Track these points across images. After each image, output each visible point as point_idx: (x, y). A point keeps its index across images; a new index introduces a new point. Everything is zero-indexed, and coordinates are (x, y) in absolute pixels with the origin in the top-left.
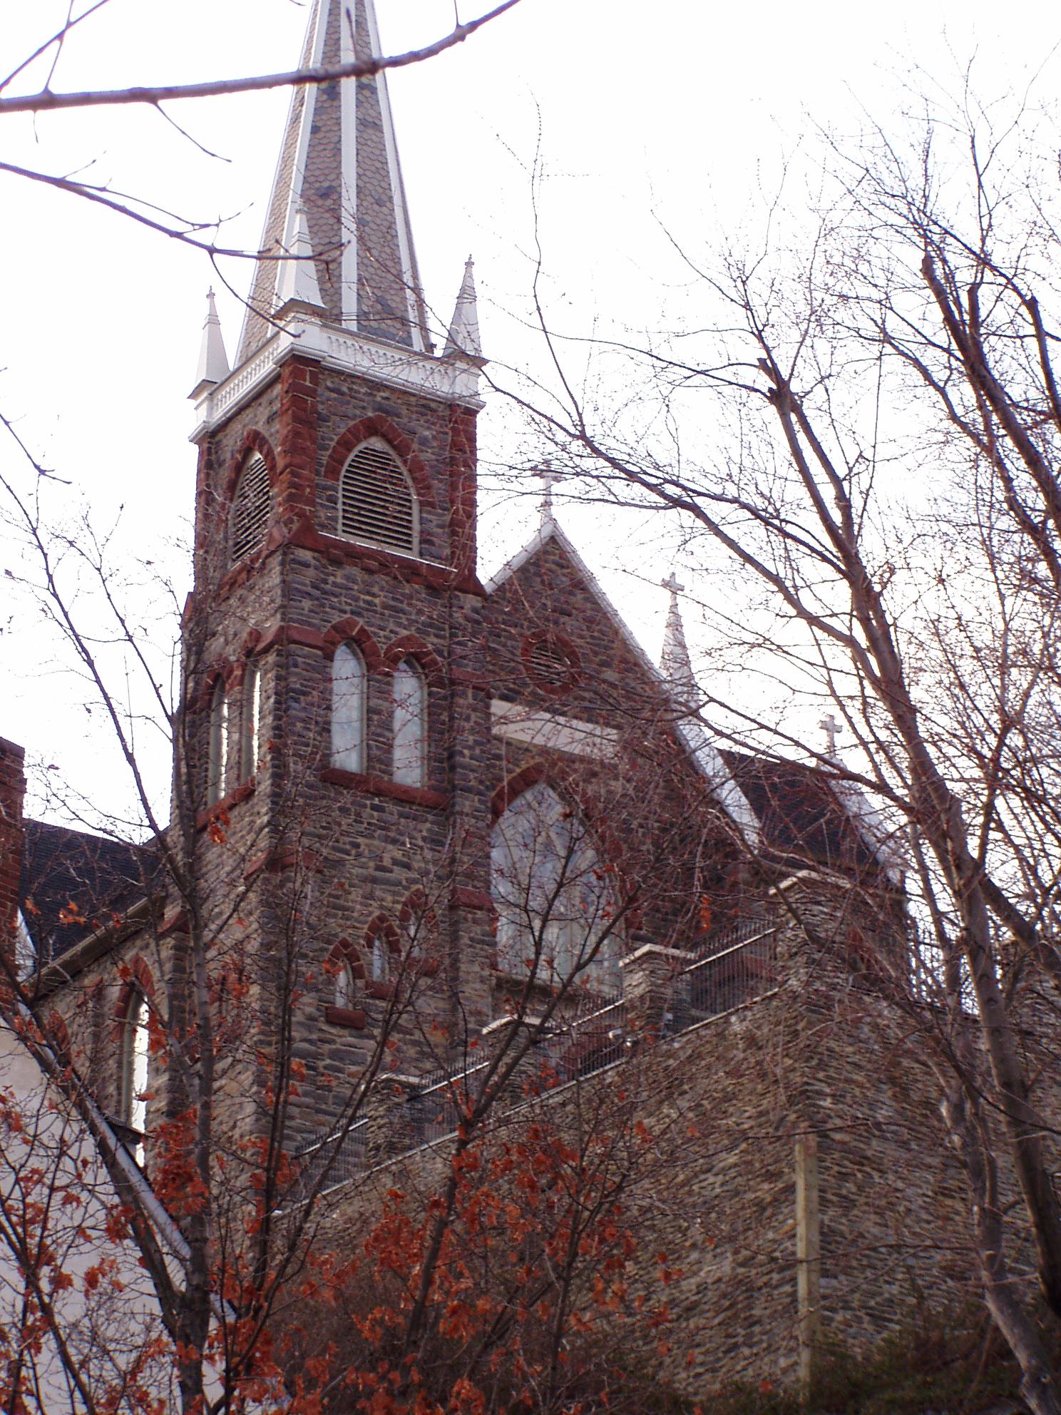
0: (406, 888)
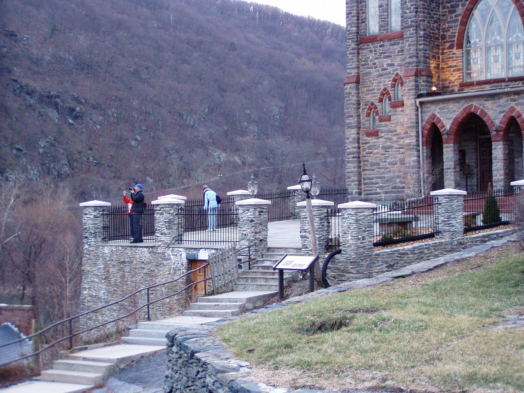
0: (392, 74)
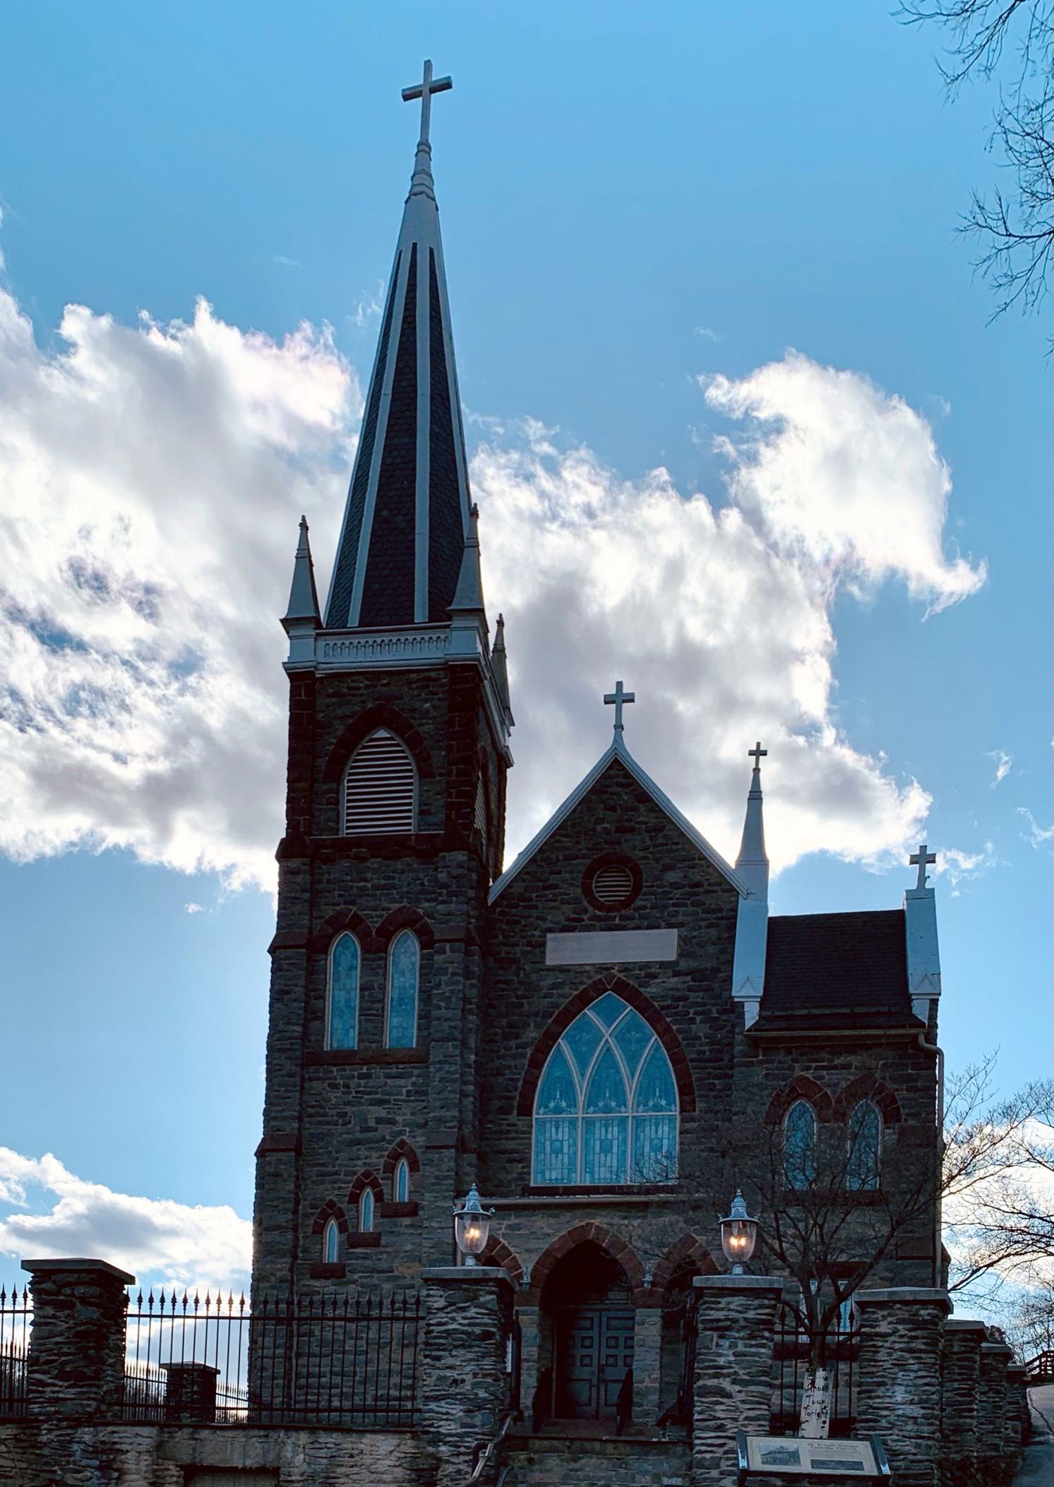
0: (389, 1142)
